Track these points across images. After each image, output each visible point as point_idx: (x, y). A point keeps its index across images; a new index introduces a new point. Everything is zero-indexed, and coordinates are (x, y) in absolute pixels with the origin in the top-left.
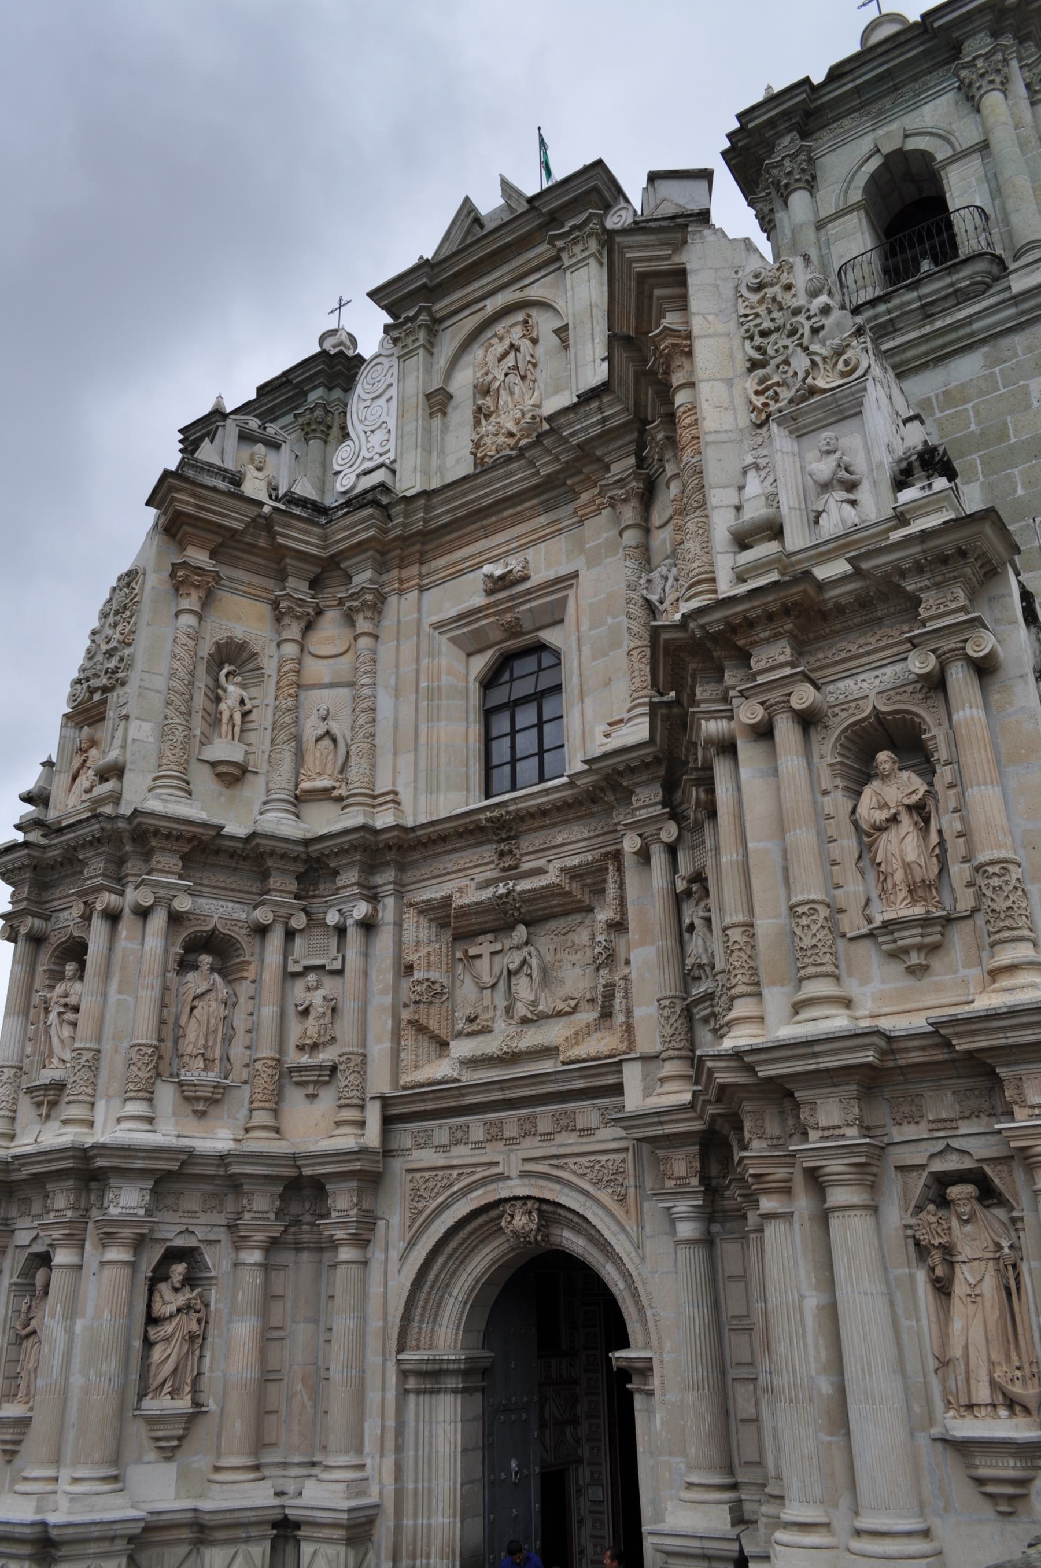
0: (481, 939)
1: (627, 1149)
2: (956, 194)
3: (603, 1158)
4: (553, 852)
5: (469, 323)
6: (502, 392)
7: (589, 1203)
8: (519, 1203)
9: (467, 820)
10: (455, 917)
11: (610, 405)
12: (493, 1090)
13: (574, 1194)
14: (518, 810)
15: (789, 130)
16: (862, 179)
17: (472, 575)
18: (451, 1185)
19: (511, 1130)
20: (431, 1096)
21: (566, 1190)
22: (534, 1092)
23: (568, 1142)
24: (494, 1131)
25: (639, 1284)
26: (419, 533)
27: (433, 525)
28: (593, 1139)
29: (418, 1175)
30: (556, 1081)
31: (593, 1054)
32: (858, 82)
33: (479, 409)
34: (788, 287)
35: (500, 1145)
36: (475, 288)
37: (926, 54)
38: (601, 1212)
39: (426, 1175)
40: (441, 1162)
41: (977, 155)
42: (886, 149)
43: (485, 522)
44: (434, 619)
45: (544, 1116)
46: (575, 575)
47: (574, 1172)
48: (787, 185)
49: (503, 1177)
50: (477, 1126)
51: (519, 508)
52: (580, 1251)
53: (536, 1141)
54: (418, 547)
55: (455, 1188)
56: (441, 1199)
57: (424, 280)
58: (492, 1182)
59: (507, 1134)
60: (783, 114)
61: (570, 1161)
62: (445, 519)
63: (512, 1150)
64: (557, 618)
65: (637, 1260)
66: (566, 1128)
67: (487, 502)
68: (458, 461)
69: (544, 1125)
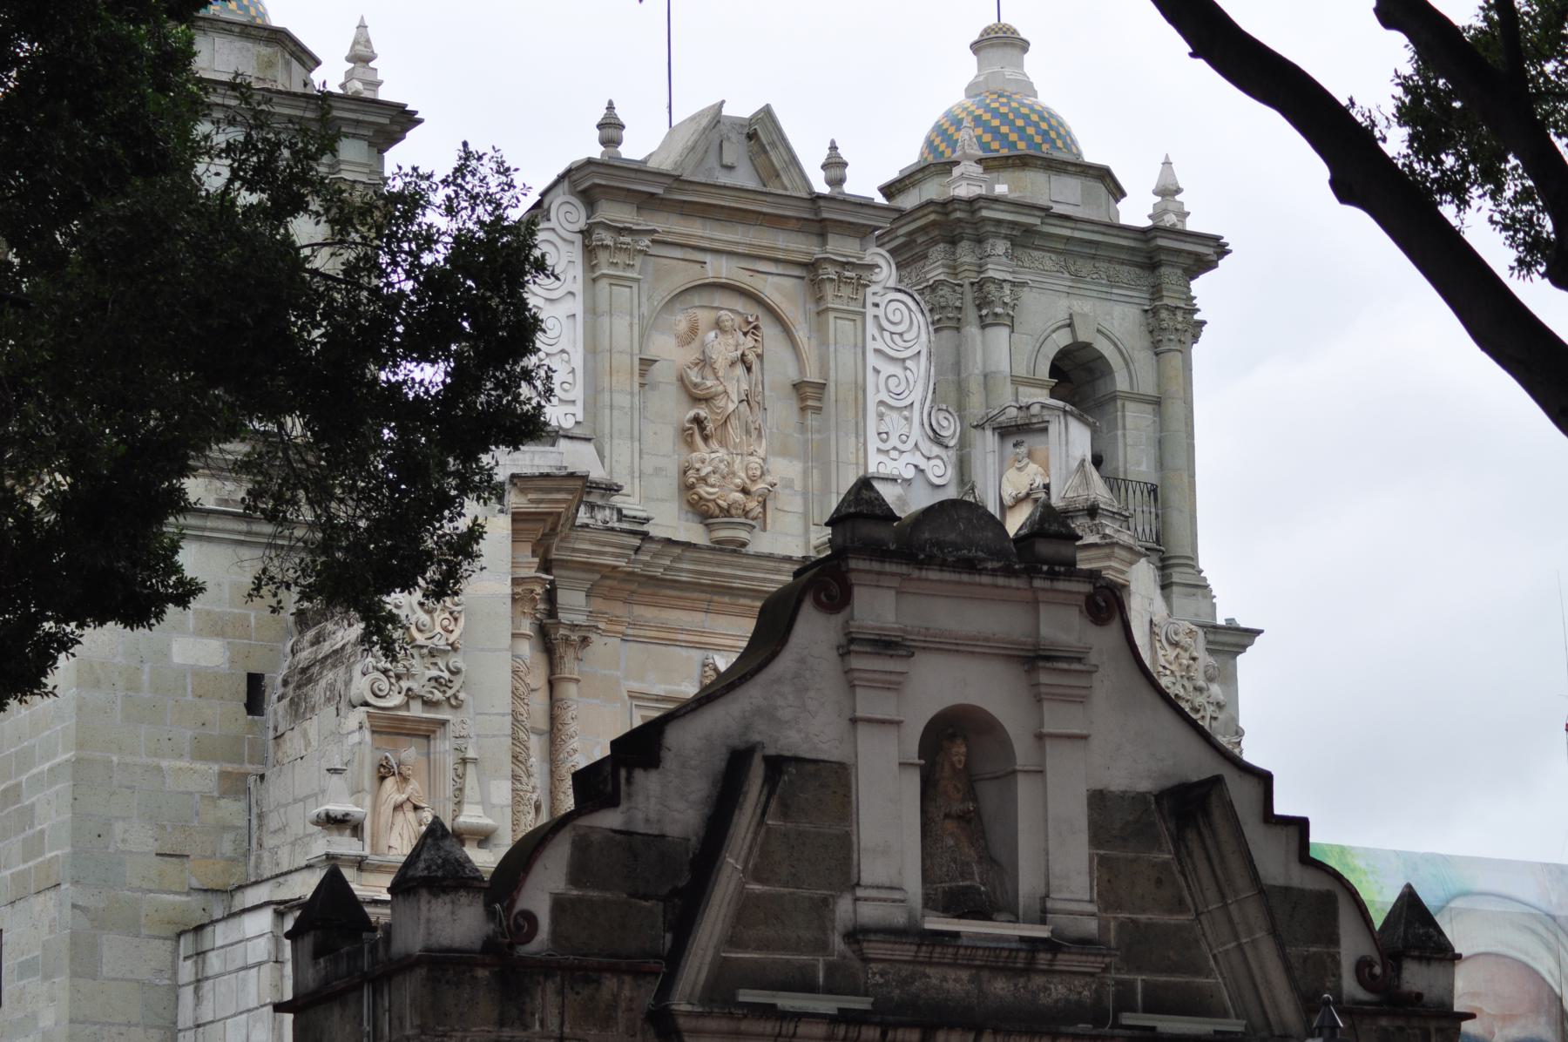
2: (1129, 441)
5: (686, 275)
6: (734, 421)
15: (1006, 237)
16: (1050, 352)
17: (684, 652)
32: (1078, 234)
33: (697, 420)
34: (1194, 659)
36: (697, 230)
37: (1133, 249)
41: (1149, 408)
42: (1083, 337)
43: (716, 598)
44: (636, 686)
48: (996, 315)
54: (634, 587)
57: (660, 191)
60: (1015, 223)
62: (684, 577)
67: (737, 584)
68: (658, 471)
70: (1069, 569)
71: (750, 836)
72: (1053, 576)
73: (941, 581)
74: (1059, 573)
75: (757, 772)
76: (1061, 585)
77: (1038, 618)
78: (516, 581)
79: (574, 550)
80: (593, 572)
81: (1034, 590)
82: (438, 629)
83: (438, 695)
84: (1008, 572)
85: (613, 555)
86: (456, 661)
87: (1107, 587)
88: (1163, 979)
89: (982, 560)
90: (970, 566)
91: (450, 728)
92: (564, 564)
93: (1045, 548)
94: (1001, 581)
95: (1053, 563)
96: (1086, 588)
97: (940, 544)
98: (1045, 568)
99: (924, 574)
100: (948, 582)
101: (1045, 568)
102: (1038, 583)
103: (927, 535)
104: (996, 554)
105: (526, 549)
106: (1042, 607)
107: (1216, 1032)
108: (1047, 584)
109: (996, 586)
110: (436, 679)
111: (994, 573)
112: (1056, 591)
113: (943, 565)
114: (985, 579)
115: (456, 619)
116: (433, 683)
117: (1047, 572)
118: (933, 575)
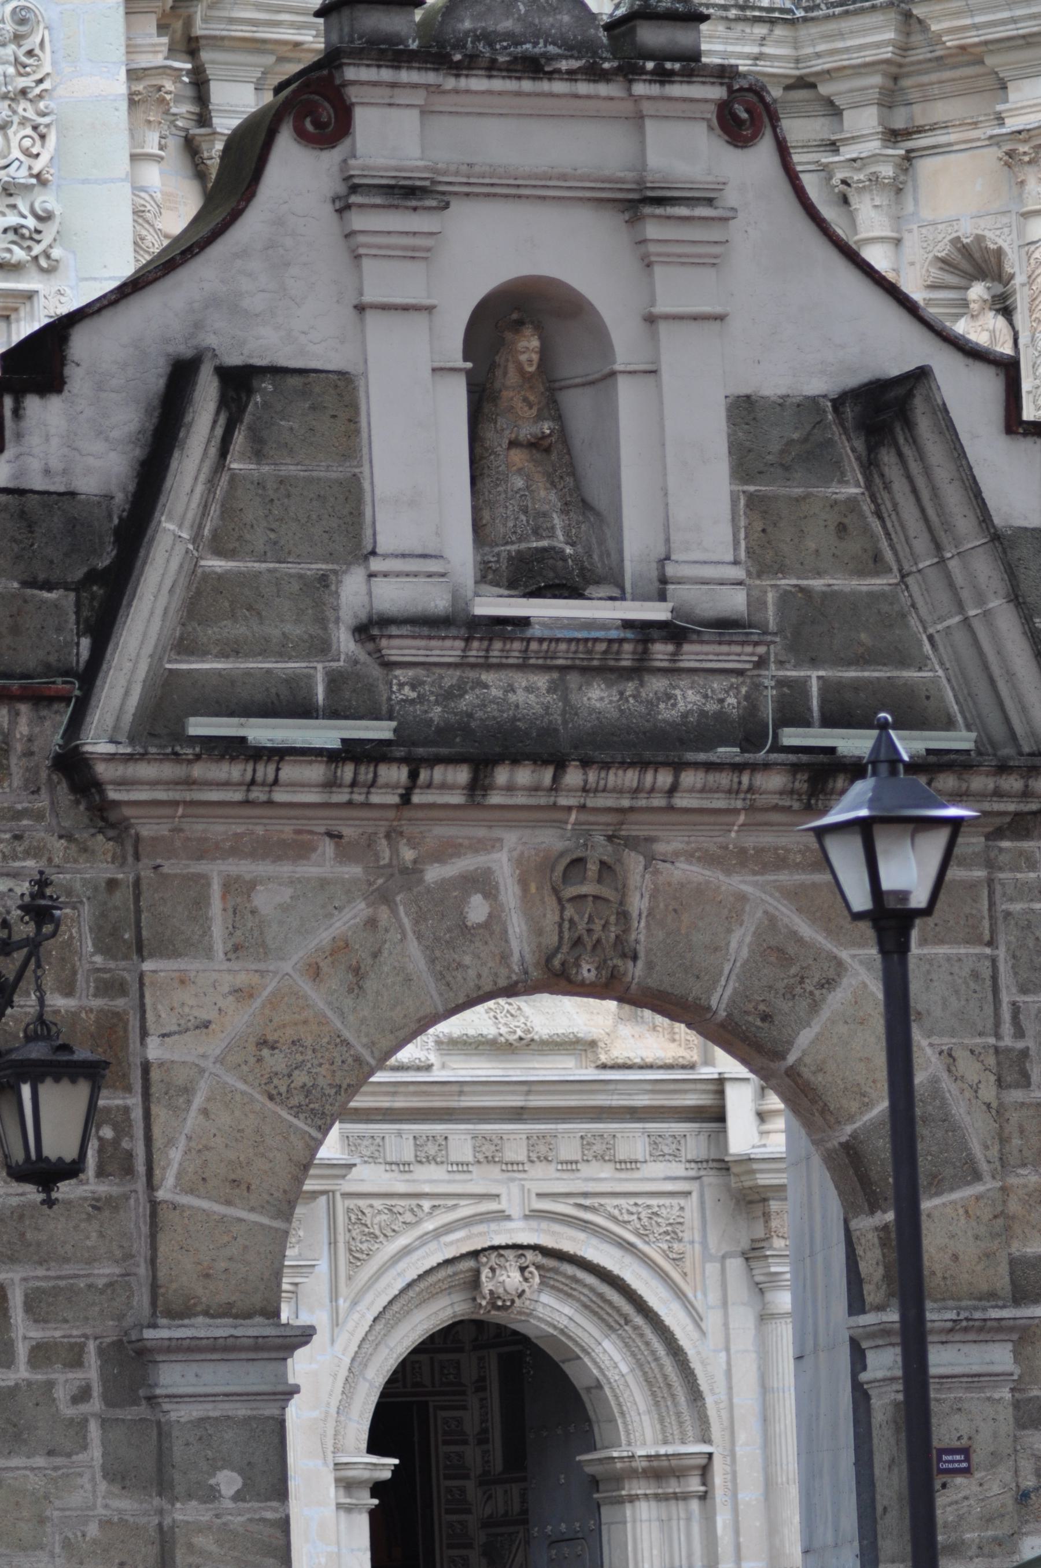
1: (688, 1193)
3: (654, 1202)
7: (628, 1259)
8: (510, 1254)
11: (778, 42)
12: (513, 1093)
13: (606, 1247)
18: (418, 1222)
19: (516, 1151)
20: (412, 1088)
21: (594, 1241)
22: (573, 1103)
23: (600, 1176)
24: (488, 1149)
25: (695, 1365)
28: (636, 1175)
29: (362, 1203)
30: (613, 1092)
31: (649, 1060)
35: (495, 1171)
38: (645, 1273)
39: (378, 1203)
40: (402, 1188)
45: (568, 1138)
47: (614, 1219)
49: (502, 1216)
50: (461, 1140)
52: (564, 1322)
53: (550, 1170)
55: (429, 1226)
56: (402, 1241)
58: (481, 1222)
59: (509, 1155)
61: (609, 1203)
63: (513, 1180)
65: (696, 1335)
66: (600, 1158)
69: (569, 1150)
70: (690, 64)
71: (200, 488)
72: (663, 76)
73: (490, 92)
74: (672, 73)
75: (207, 391)
76: (676, 90)
77: (643, 142)
78: (133, 75)
79: (232, 21)
80: (264, 52)
81: (637, 99)
82: (16, 153)
83: (19, 254)
84: (594, 74)
85: (293, 25)
86: (46, 200)
87: (750, 90)
88: (852, 674)
89: (551, 58)
90: (533, 67)
91: (40, 302)
92: (217, 42)
93: (652, 36)
94: (583, 88)
95: (661, 56)
96: (717, 92)
97: (488, 38)
98: (650, 65)
99: (463, 83)
100: (500, 93)
101: (650, 65)
102: (640, 89)
103: (467, 25)
104: (573, 48)
105: (150, 24)
106: (650, 125)
107: (929, 751)
108: (655, 90)
109: (577, 96)
110: (16, 230)
111: (571, 75)
112: (670, 99)
113: (492, 68)
114: (559, 87)
115: (43, 137)
116: (11, 236)
117: (652, 73)
118: (477, 83)
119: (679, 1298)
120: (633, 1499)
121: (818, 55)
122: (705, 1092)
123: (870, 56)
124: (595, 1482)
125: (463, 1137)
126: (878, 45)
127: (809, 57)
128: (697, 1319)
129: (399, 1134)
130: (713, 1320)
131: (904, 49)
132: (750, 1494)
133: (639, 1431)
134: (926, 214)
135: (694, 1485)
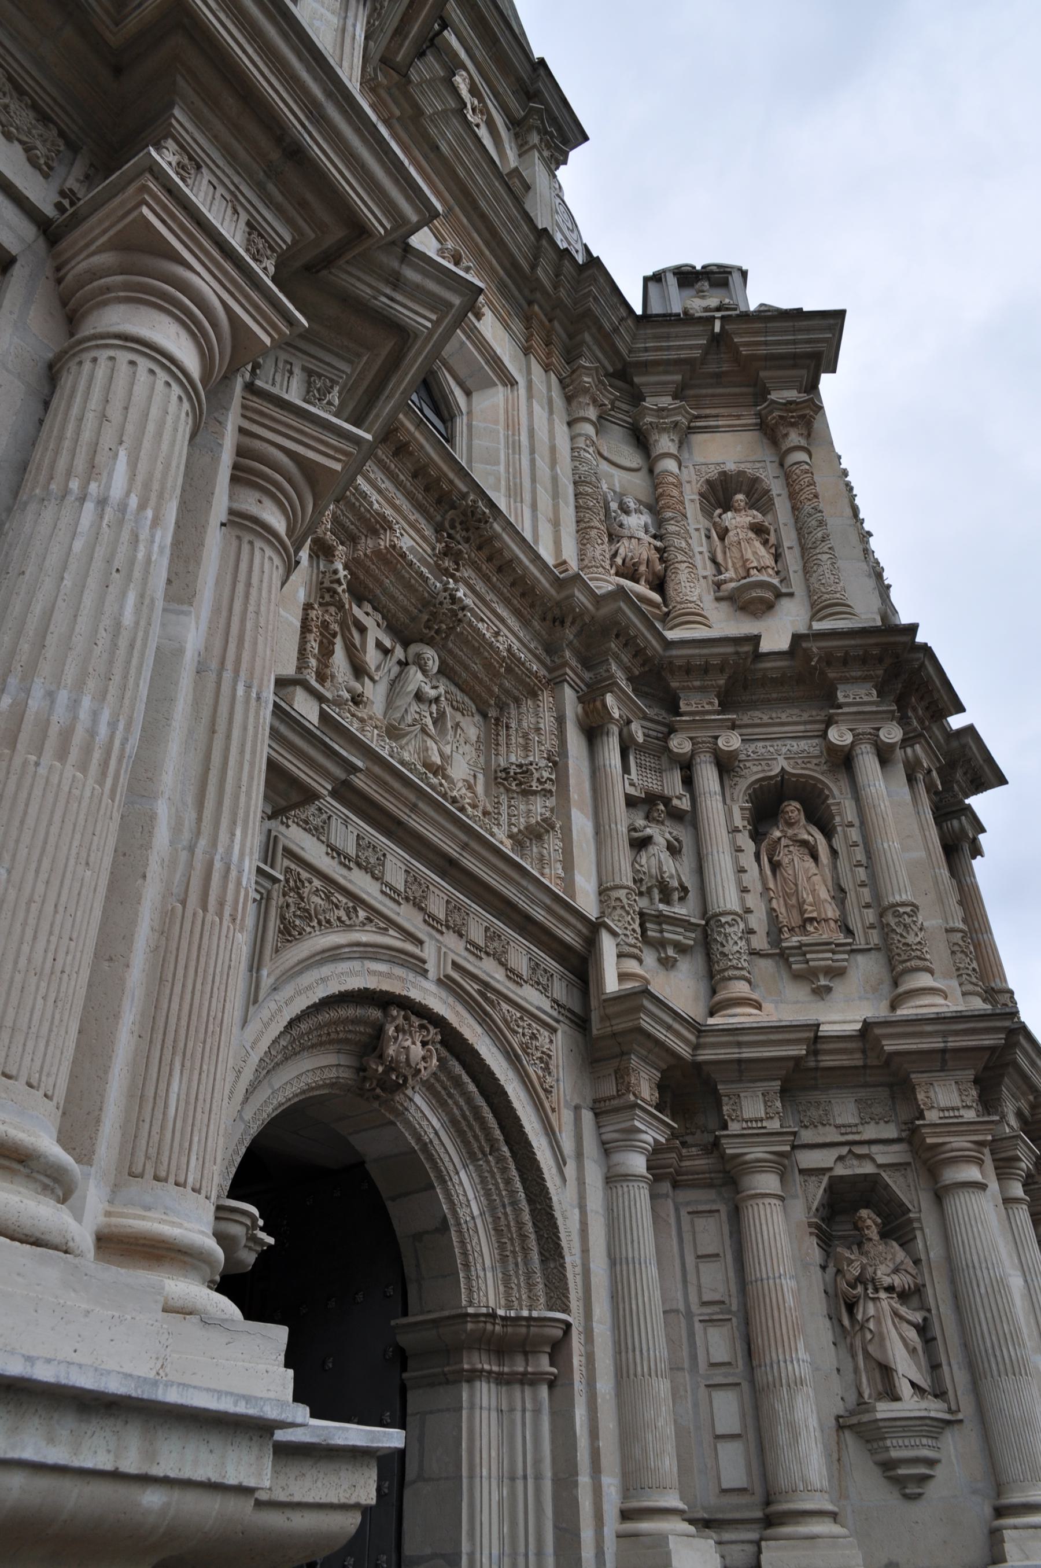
0: (369, 608)
4: (489, 614)
9: (451, 475)
10: (377, 552)
14: (498, 537)
24: (416, 891)
26: (419, 112)
27: (432, 131)
46: (512, 383)
50: (397, 864)
51: (487, 252)
54: (397, 113)
64: (469, 383)
67: (483, 204)
119: (547, 1135)
120: (474, 1376)
121: (646, 349)
122: (579, 933)
123: (684, 354)
124: (402, 1358)
125: (399, 864)
126: (691, 347)
127: (639, 350)
128: (560, 1162)
129: (346, 822)
130: (570, 1170)
131: (703, 360)
132: (605, 1386)
133: (487, 1289)
134: (699, 458)
135: (544, 1364)
